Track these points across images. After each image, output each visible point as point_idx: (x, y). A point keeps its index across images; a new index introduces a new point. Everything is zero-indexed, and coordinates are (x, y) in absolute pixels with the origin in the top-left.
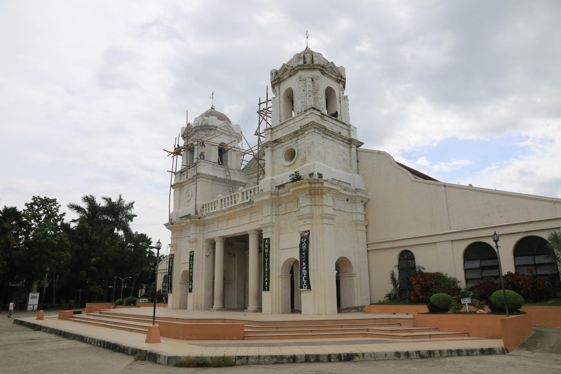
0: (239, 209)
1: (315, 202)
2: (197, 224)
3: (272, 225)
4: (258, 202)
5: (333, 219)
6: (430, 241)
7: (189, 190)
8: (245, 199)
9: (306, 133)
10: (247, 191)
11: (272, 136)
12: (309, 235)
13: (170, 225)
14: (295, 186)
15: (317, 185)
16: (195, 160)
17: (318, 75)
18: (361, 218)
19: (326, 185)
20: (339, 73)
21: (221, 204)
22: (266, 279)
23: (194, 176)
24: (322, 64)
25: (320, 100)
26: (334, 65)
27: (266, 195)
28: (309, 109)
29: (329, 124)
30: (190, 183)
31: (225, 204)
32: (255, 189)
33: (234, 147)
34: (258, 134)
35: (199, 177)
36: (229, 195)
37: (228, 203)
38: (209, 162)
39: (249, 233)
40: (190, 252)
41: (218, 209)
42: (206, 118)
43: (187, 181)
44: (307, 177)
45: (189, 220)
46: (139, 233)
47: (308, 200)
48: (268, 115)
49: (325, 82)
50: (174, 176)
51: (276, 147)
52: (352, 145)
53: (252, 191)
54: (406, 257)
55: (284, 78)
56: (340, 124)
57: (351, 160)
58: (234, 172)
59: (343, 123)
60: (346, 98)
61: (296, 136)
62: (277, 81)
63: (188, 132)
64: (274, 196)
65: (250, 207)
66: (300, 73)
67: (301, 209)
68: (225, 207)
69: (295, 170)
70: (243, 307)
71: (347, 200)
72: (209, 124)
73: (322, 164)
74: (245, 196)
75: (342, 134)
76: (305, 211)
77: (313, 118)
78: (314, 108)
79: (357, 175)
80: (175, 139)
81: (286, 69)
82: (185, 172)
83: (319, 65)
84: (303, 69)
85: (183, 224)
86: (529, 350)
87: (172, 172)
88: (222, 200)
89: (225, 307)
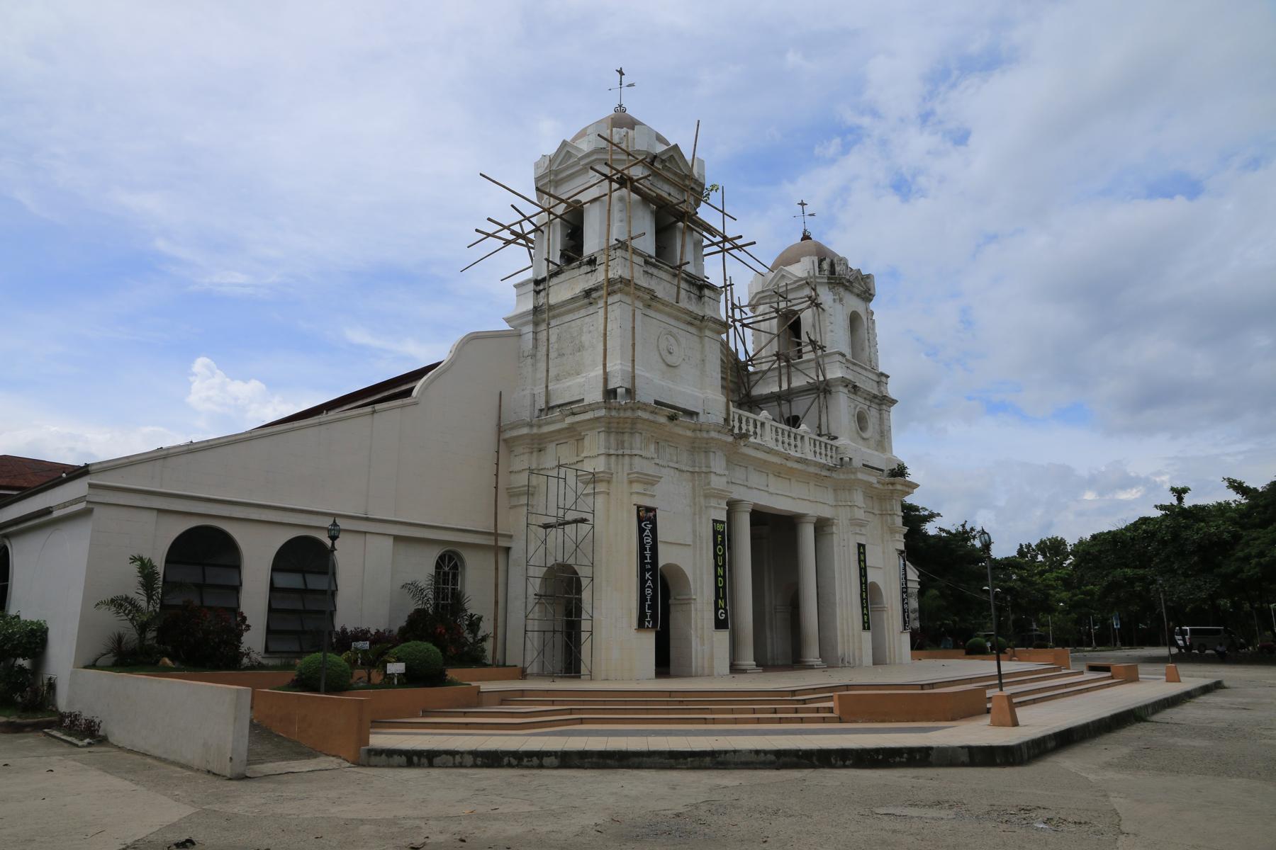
0: (812, 469)
23: (621, 280)
30: (677, 318)
43: (672, 306)
46: (1087, 536)
77: (618, 269)
89: (764, 664)
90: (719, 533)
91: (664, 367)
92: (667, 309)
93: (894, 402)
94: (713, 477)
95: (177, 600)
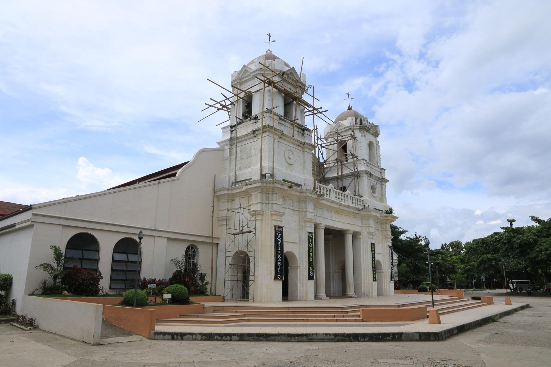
0: (351, 210)
23: (269, 126)
30: (293, 143)
46: (471, 241)
77: (267, 122)
89: (330, 295)
90: (310, 238)
91: (287, 165)
92: (289, 139)
93: (387, 181)
94: (308, 213)
95: (70, 265)
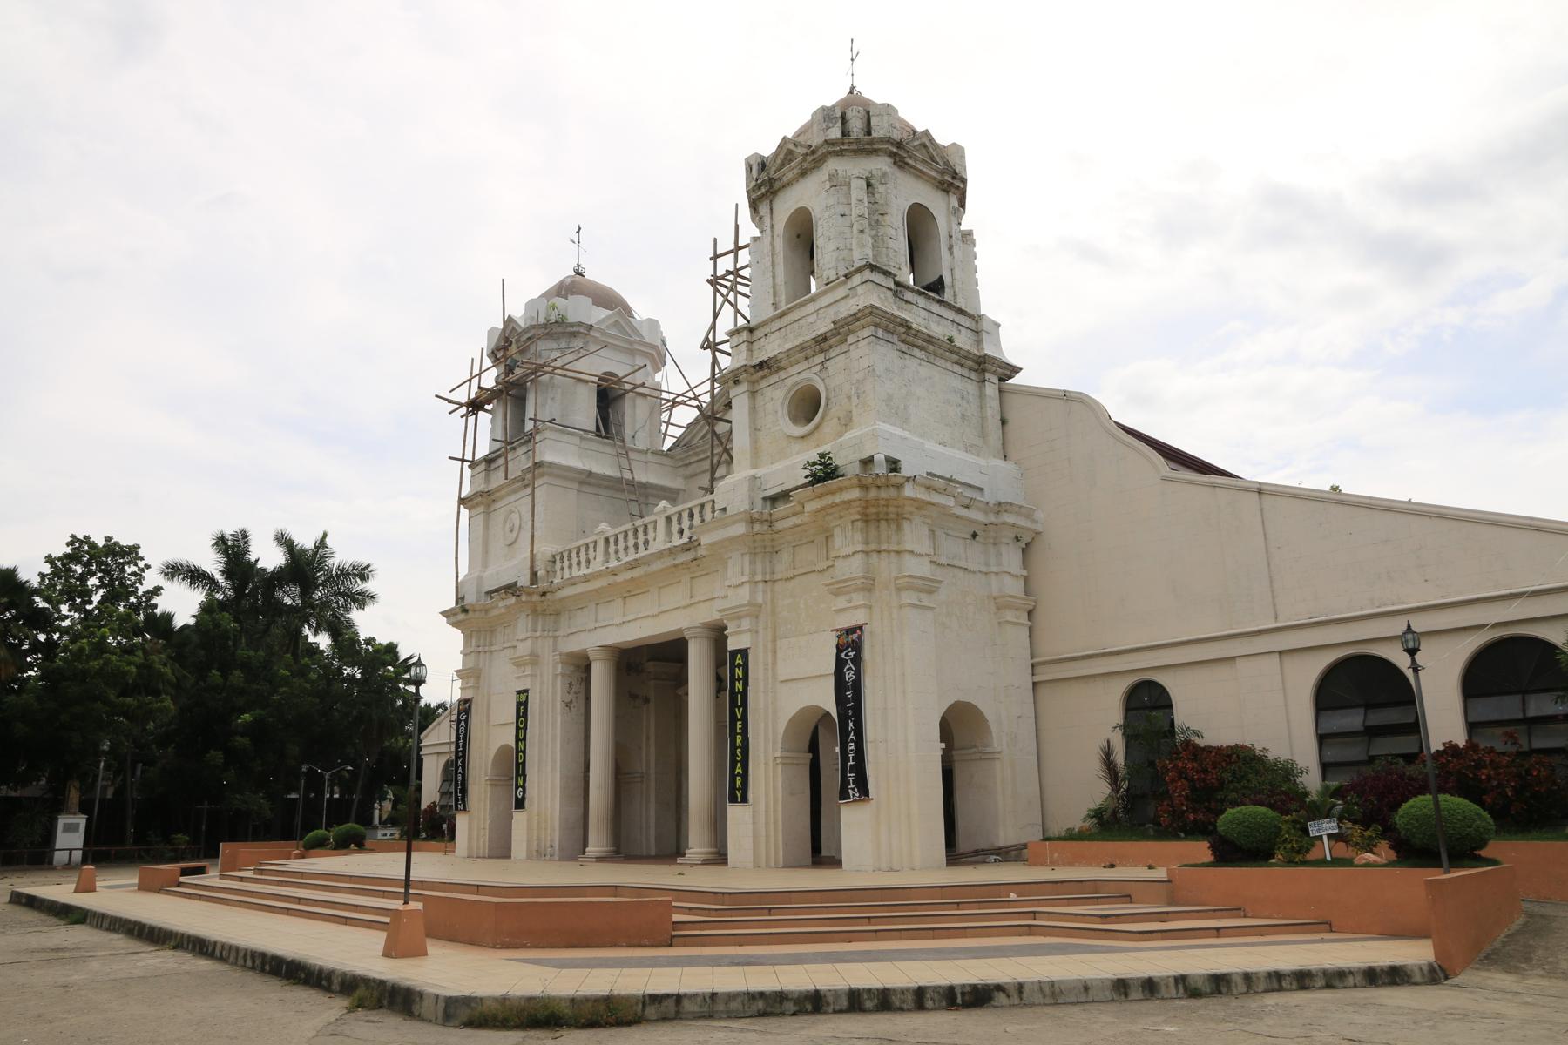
0: (657, 566)
1: (879, 543)
2: (535, 612)
3: (754, 611)
4: (711, 545)
5: (930, 592)
6: (1219, 651)
7: (511, 512)
8: (676, 535)
9: (851, 339)
10: (680, 514)
11: (750, 350)
12: (860, 638)
13: (460, 614)
14: (821, 496)
15: (883, 494)
16: (529, 426)
17: (886, 168)
18: (1014, 587)
19: (909, 491)
20: (947, 163)
21: (607, 552)
22: (739, 769)
24: (896, 136)
25: (891, 244)
26: (931, 140)
27: (735, 522)
28: (859, 270)
29: (919, 314)
30: (515, 491)
31: (617, 552)
32: (702, 506)
33: (643, 385)
34: (710, 345)
35: (542, 475)
36: (628, 526)
37: (626, 549)
38: (568, 429)
39: (687, 635)
40: (519, 692)
41: (598, 565)
42: (560, 302)
43: (508, 485)
44: (855, 469)
45: (513, 600)
47: (858, 537)
48: (740, 288)
49: (904, 192)
50: (467, 472)
51: (763, 384)
52: (987, 376)
53: (696, 512)
54: (1147, 702)
55: (785, 179)
56: (950, 315)
57: (983, 418)
58: (642, 457)
59: (961, 311)
60: (967, 236)
61: (822, 351)
62: (763, 190)
63: (509, 346)
64: (757, 527)
65: (691, 559)
66: (833, 165)
67: (838, 563)
68: (618, 559)
69: (821, 450)
70: (671, 851)
71: (974, 535)
72: (571, 319)
73: (898, 431)
74: (675, 528)
75: (957, 343)
76: (852, 568)
78: (873, 268)
79: (1001, 463)
80: (465, 360)
81: (790, 152)
82: (501, 461)
83: (889, 140)
84: (841, 153)
85: (495, 612)
86: (1508, 971)
87: (463, 460)
88: (607, 540)
89: (622, 850)
